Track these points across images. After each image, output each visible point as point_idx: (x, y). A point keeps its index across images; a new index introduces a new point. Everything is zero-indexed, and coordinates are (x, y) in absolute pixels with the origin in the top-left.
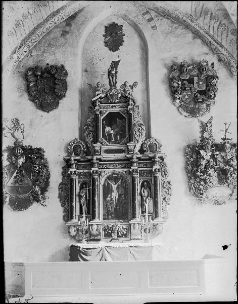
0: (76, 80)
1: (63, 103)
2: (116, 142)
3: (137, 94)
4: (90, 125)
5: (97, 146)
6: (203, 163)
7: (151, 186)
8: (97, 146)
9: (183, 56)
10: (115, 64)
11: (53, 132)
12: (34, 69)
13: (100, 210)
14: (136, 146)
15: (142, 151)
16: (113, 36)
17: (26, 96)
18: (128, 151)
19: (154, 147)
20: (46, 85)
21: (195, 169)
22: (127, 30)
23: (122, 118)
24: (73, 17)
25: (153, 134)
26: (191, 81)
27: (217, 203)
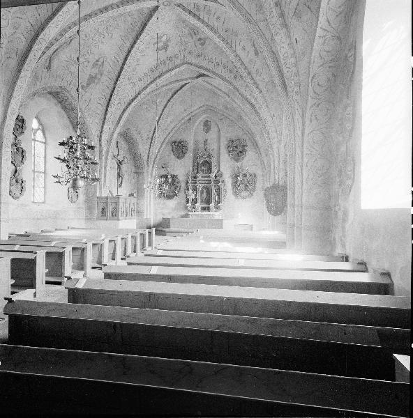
0: (191, 146)
1: (186, 155)
2: (206, 173)
3: (215, 154)
4: (197, 167)
5: (198, 175)
6: (239, 183)
7: (218, 190)
8: (198, 175)
9: (233, 136)
10: (205, 142)
11: (181, 168)
12: (175, 142)
13: (199, 200)
14: (213, 175)
15: (216, 176)
16: (207, 125)
17: (172, 152)
18: (209, 177)
19: (221, 175)
20: (179, 148)
21: (235, 185)
22: (213, 124)
23: (208, 163)
24: (190, 119)
25: (221, 169)
26: (236, 147)
27: (244, 198)
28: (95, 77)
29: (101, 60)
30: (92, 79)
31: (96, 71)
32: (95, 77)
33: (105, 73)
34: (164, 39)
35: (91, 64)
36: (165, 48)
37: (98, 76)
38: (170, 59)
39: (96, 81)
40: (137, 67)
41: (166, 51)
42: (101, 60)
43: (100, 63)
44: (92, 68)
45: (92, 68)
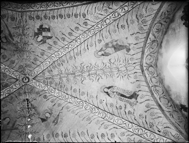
28: (113, 46)
29: (100, 53)
30: (117, 48)
31: (110, 50)
32: (113, 46)
33: (103, 43)
34: (40, 38)
35: (109, 57)
36: (41, 29)
37: (110, 45)
38: (38, 17)
39: (115, 43)
40: (73, 28)
41: (41, 26)
42: (100, 53)
43: (103, 52)
44: (110, 54)
45: (110, 54)
